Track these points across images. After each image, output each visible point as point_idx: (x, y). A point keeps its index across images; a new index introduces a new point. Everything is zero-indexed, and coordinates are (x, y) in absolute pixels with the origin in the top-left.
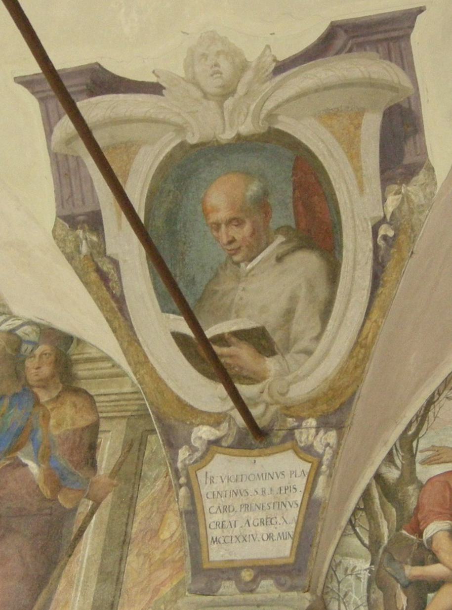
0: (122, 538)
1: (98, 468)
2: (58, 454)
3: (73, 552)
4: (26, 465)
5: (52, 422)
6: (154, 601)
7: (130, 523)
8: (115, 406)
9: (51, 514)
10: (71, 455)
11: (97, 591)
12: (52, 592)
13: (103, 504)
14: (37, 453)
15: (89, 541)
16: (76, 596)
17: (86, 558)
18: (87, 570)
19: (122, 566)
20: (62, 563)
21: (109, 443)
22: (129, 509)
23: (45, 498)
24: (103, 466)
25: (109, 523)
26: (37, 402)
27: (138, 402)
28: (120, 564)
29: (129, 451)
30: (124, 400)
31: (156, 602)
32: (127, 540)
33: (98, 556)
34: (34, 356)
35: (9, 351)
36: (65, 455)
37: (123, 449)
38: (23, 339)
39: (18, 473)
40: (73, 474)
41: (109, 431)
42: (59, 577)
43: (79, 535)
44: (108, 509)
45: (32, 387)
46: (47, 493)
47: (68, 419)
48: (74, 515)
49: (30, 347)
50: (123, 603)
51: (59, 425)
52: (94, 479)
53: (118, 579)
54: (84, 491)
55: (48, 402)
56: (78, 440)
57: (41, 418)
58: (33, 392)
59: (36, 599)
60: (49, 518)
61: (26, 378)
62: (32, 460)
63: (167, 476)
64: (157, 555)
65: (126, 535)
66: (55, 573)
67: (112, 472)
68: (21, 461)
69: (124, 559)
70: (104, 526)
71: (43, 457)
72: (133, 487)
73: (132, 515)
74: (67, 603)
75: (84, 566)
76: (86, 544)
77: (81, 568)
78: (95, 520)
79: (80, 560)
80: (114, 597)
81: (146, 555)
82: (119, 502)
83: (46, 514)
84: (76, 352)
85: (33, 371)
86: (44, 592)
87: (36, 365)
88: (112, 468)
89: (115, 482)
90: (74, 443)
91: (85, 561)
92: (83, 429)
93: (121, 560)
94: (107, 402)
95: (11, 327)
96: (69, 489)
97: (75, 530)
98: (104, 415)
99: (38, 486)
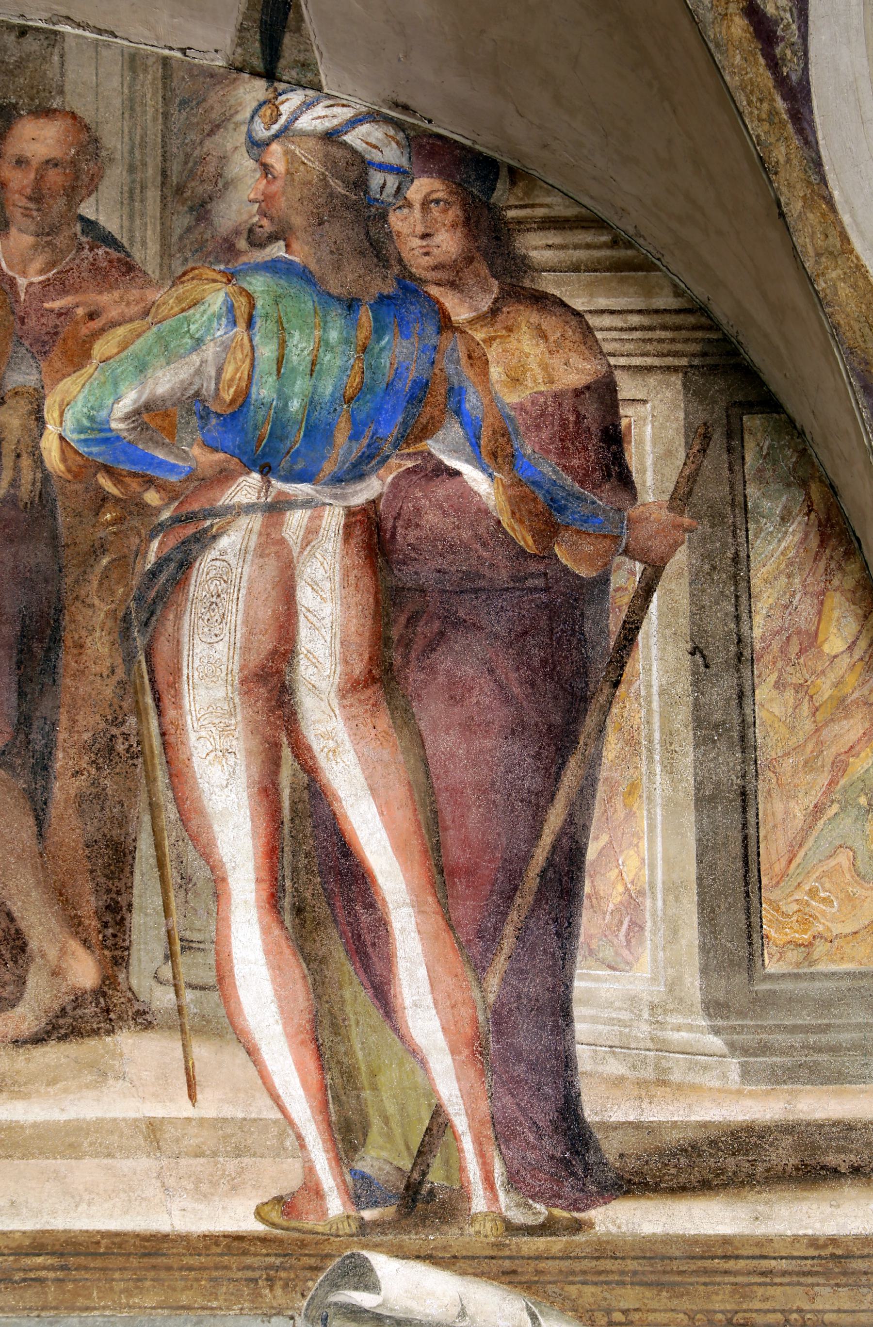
0: (733, 649)
1: (638, 486)
2: (529, 452)
3: (621, 675)
4: (457, 473)
5: (495, 372)
6: (839, 787)
7: (745, 616)
8: (644, 341)
9: (547, 589)
10: (563, 452)
11: (699, 763)
12: (593, 762)
13: (670, 569)
14: (476, 445)
15: (654, 651)
16: (651, 773)
17: (655, 690)
18: (665, 719)
19: (748, 711)
20: (602, 699)
21: (649, 429)
22: (736, 584)
23: (524, 552)
24: (649, 482)
25: (693, 614)
26: (445, 324)
27: (700, 334)
28: (740, 705)
29: (703, 451)
30: (664, 328)
31: (845, 790)
32: (747, 653)
33: (683, 685)
34: (410, 205)
35: (340, 188)
36: (548, 452)
37: (689, 446)
38: (367, 157)
39: (442, 489)
40: (579, 498)
41: (644, 402)
42: (601, 729)
43: (625, 638)
44: (685, 580)
45: (422, 281)
46: (526, 540)
47: (534, 366)
48: (605, 592)
49: (392, 181)
50: (769, 792)
51: (515, 381)
52: (633, 512)
53: (743, 738)
54: (617, 538)
55: (471, 322)
56: (572, 418)
57: (464, 360)
58: (428, 297)
59: (558, 778)
60: (544, 597)
61: (400, 260)
62: (467, 461)
63: (810, 511)
64: (825, 689)
65: (740, 641)
66: (590, 722)
67: (672, 498)
68: (441, 463)
69: (748, 693)
70: (684, 621)
71: (494, 455)
72: (735, 536)
73: (744, 599)
74: (633, 788)
75: (655, 705)
76: (648, 658)
77: (649, 711)
78: (659, 606)
79: (643, 693)
80: (744, 776)
81: (798, 688)
82: (707, 567)
83: (536, 589)
84: (513, 202)
85: (417, 242)
86: (572, 763)
87: (420, 229)
88: (671, 488)
89: (686, 521)
90: (564, 425)
91: (655, 698)
92: (578, 393)
93: (741, 696)
94: (621, 329)
95: (328, 124)
96: (578, 532)
97: (614, 625)
98: (622, 361)
99: (499, 522)
